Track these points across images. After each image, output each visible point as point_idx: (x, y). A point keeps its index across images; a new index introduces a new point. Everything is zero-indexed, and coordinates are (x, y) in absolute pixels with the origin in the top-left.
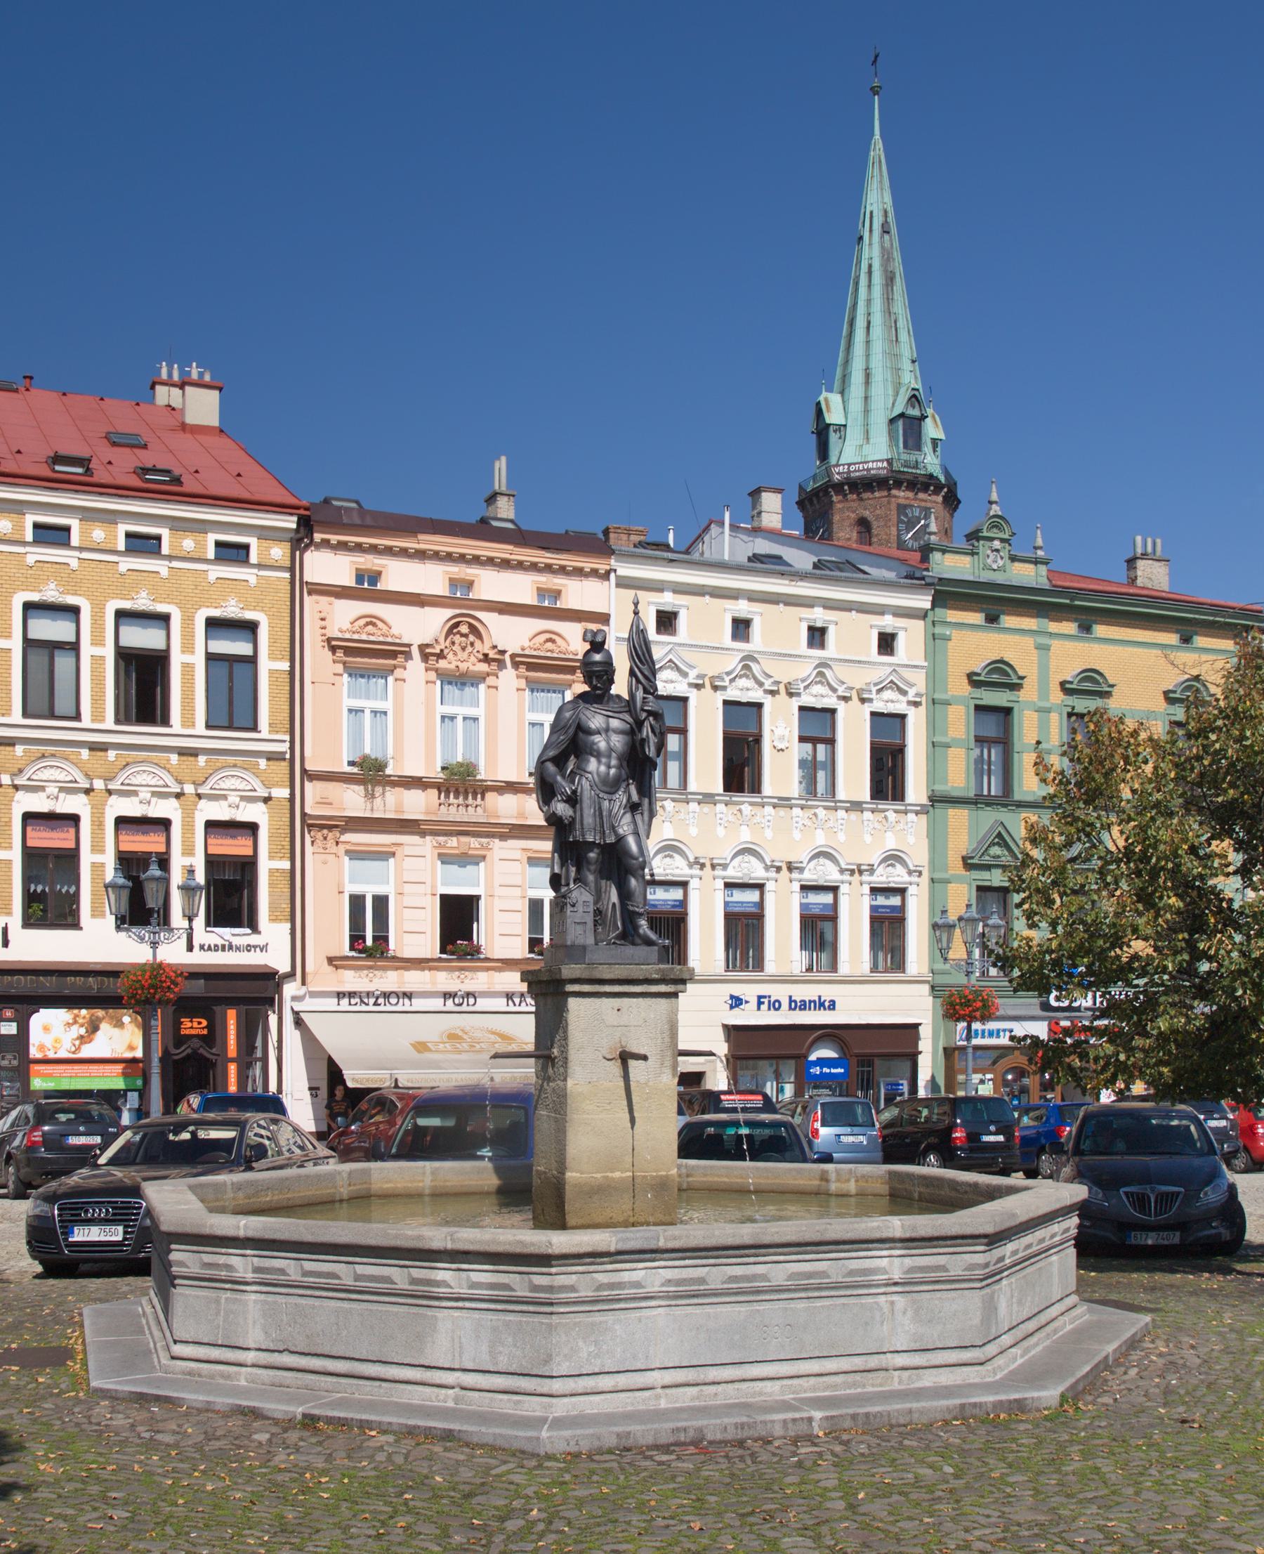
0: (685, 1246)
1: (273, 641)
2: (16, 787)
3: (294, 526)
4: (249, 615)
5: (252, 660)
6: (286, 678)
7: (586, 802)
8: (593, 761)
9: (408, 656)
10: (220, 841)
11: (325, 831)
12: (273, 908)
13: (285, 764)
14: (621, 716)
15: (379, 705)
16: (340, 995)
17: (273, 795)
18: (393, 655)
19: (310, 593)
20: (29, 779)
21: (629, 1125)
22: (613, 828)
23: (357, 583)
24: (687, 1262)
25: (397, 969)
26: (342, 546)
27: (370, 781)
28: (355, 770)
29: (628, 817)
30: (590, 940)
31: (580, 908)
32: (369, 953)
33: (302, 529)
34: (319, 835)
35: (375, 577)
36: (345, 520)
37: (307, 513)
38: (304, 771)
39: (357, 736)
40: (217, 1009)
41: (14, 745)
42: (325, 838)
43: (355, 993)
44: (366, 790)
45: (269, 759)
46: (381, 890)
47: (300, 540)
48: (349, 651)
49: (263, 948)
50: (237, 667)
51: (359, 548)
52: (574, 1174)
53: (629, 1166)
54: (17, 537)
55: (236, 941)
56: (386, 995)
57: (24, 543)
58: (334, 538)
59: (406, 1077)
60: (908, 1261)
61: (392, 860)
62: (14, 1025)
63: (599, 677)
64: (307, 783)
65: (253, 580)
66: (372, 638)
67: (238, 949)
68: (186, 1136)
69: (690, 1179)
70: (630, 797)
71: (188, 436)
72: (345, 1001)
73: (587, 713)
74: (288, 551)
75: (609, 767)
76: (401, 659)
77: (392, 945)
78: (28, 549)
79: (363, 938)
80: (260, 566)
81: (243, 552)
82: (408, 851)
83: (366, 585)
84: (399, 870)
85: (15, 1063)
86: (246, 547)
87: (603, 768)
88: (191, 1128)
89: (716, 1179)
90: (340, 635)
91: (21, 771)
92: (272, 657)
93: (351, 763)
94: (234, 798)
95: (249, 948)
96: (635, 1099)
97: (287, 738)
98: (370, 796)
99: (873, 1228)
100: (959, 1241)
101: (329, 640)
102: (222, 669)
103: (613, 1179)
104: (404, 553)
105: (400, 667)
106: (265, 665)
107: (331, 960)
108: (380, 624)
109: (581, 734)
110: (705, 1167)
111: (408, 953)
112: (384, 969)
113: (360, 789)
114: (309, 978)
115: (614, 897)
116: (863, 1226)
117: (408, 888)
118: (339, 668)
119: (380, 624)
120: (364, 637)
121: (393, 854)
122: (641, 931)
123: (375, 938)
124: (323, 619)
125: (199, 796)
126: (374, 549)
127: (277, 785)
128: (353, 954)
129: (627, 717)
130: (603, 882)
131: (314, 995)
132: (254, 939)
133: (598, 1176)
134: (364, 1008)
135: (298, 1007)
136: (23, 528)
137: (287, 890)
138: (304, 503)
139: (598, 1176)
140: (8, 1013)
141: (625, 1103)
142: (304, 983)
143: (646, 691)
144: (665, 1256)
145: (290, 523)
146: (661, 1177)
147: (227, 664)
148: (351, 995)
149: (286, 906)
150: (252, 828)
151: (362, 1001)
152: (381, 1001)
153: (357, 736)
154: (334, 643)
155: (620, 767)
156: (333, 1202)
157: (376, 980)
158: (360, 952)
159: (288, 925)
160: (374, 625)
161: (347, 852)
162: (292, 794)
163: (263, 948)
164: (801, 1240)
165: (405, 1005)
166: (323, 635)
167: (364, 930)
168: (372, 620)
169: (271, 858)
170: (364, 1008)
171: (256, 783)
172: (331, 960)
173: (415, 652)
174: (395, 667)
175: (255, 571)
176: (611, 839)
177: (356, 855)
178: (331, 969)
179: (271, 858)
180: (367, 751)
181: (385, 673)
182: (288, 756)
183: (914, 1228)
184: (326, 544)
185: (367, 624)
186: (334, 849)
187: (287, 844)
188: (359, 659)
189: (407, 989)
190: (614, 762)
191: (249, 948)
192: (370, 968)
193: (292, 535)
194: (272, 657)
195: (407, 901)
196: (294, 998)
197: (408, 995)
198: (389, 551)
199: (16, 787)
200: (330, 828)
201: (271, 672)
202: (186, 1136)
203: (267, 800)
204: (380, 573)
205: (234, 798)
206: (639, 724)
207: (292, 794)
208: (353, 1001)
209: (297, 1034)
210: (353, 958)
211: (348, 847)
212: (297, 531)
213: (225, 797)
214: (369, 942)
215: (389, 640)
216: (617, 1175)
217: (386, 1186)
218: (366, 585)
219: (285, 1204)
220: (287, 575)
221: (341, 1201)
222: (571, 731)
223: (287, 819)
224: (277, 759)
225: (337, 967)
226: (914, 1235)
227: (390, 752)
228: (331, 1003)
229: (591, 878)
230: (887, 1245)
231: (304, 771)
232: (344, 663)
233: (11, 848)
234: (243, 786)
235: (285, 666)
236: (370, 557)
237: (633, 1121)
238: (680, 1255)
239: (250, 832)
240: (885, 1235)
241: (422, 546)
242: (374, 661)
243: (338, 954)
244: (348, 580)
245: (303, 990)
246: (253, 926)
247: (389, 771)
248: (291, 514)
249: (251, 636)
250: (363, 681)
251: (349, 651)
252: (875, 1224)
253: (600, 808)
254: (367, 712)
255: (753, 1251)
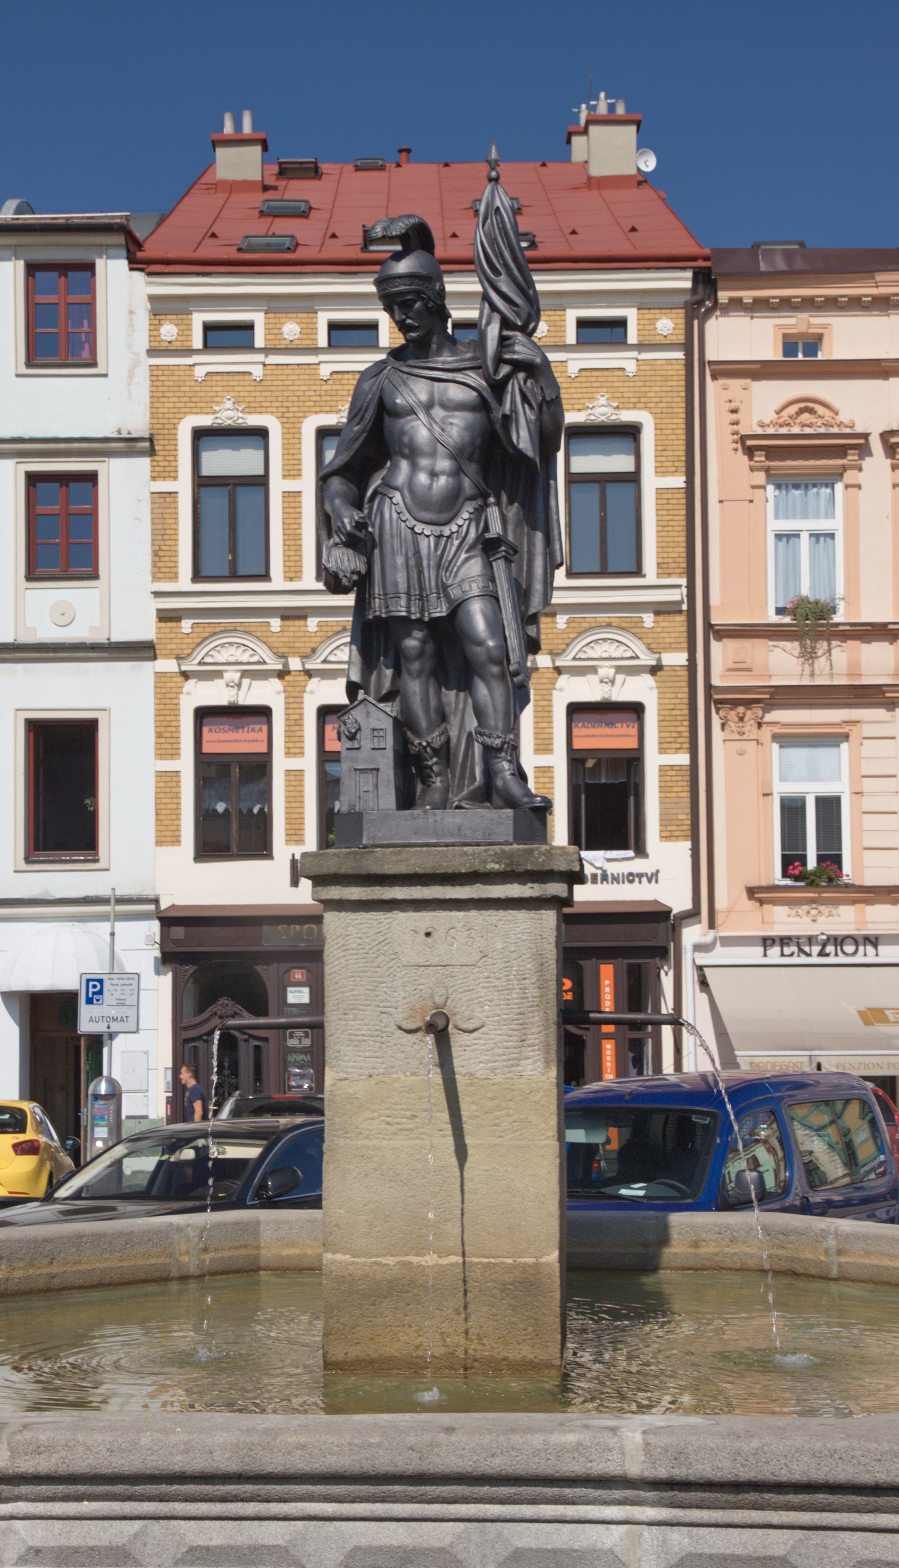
0: (63, 1469)
1: (661, 448)
2: (309, 674)
3: (688, 284)
4: (627, 416)
5: (633, 479)
6: (681, 498)
7: (391, 543)
8: (404, 465)
9: (864, 450)
10: (591, 731)
11: (741, 709)
12: (664, 821)
13: (681, 619)
14: (459, 377)
15: (822, 525)
16: (767, 942)
17: (665, 662)
18: (841, 451)
19: (714, 377)
20: (325, 661)
21: (454, 1161)
22: (443, 588)
23: (785, 354)
24: (87, 1507)
25: (854, 902)
26: (761, 306)
27: (807, 634)
28: (787, 620)
29: (475, 567)
30: (388, 799)
31: (366, 741)
32: (809, 880)
33: (701, 288)
34: (732, 715)
35: (813, 343)
36: (763, 267)
37: (707, 264)
38: (708, 626)
39: (790, 571)
40: (586, 964)
41: (305, 618)
42: (741, 719)
43: (789, 938)
44: (803, 646)
45: (657, 613)
46: (828, 789)
47: (700, 303)
48: (772, 452)
49: (653, 877)
50: (611, 488)
51: (786, 305)
52: (339, 1257)
53: (455, 1243)
54: (307, 343)
55: (613, 869)
56: (839, 941)
57: (315, 350)
58: (748, 295)
59: (834, 1060)
60: (679, 1538)
61: (844, 746)
62: (306, 990)
63: (406, 306)
64: (715, 645)
65: (631, 367)
66: (808, 430)
67: (616, 879)
68: (188, 1154)
69: (843, 1259)
70: (486, 529)
71: (595, 193)
72: (775, 951)
73: (396, 378)
74: (681, 321)
75: (433, 475)
76: (852, 456)
77: (847, 867)
78: (322, 357)
79: (803, 859)
80: (641, 347)
81: (618, 331)
82: (867, 730)
83: (800, 357)
84: (855, 760)
85: (307, 1042)
86: (621, 323)
87: (423, 478)
88: (200, 1142)
89: (886, 1262)
90: (759, 431)
91: (314, 650)
92: (660, 471)
93: (780, 611)
94: (607, 671)
95: (631, 878)
96: (466, 1110)
97: (683, 581)
98: (809, 655)
99: (562, 1451)
100: (822, 1498)
101: (743, 439)
102: (591, 494)
103: (420, 1266)
104: (855, 304)
105: (852, 467)
106: (650, 483)
107: (752, 892)
108: (820, 410)
109: (387, 419)
110: (866, 1237)
111: (871, 879)
112: (836, 902)
113: (793, 646)
114: (719, 919)
115: (472, 723)
116: (537, 1440)
117: (868, 785)
118: (760, 478)
119: (820, 410)
120: (796, 430)
121: (846, 737)
122: (499, 783)
123: (820, 859)
124: (734, 411)
125: (559, 670)
126: (809, 304)
127: (670, 648)
128: (788, 882)
129: (474, 379)
130: (450, 696)
131: (728, 942)
132: (638, 865)
133: (390, 1261)
134: (804, 960)
135: (702, 959)
136: (314, 331)
137: (686, 795)
138: (707, 251)
139: (390, 1261)
140: (298, 975)
141: (446, 1116)
142: (712, 925)
143: (506, 323)
144: (24, 1489)
145: (683, 281)
146: (524, 1267)
147: (596, 487)
148: (784, 941)
149: (685, 817)
150: (636, 710)
151: (801, 950)
152: (830, 949)
153: (790, 571)
154: (750, 443)
155: (457, 472)
156: (164, 1279)
157: (821, 919)
158: (797, 878)
159: (688, 844)
160: (811, 411)
161: (776, 737)
162: (692, 659)
163: (653, 877)
164: (367, 1467)
165: (869, 954)
166: (735, 433)
167: (804, 848)
168: (807, 405)
169: (662, 750)
170: (804, 960)
171: (639, 648)
172: (752, 892)
173: (876, 444)
174: (845, 468)
175: (634, 354)
176: (440, 610)
177: (785, 740)
178: (755, 904)
179: (662, 750)
180: (805, 590)
181: (830, 479)
182: (685, 607)
183: (679, 1455)
184: (736, 305)
185: (801, 411)
186: (754, 733)
187: (685, 729)
188: (789, 463)
189: (871, 930)
190: (444, 464)
191: (631, 878)
192: (812, 901)
193: (687, 297)
194: (660, 471)
195: (868, 803)
196: (698, 948)
197: (873, 941)
198: (832, 304)
199: (309, 674)
200: (748, 703)
201: (660, 491)
202: (188, 1154)
203: (655, 670)
204: (820, 337)
205: (607, 671)
206: (498, 388)
207: (692, 659)
208: (787, 950)
209: (704, 997)
210: (786, 888)
211: (776, 730)
212: (694, 290)
213: (594, 670)
214: (812, 863)
215: (835, 430)
216: (430, 1260)
217: (286, 1252)
218: (800, 357)
219: (41, 1284)
220: (680, 355)
221: (184, 1278)
222: (369, 415)
223: (684, 695)
224: (669, 613)
225: (761, 902)
226: (680, 1472)
227: (840, 591)
228: (754, 954)
229: (414, 687)
230: (618, 1494)
231: (708, 626)
232: (767, 470)
233: (302, 754)
234: (619, 652)
235: (679, 481)
236: (803, 316)
237: (461, 1153)
238: (61, 1489)
239: (634, 716)
240: (598, 1467)
241: (883, 291)
242: (812, 462)
243: (763, 883)
244: (771, 351)
245: (710, 936)
246: (641, 851)
247: (837, 618)
248: (683, 269)
249: (632, 446)
250: (797, 493)
251: (772, 452)
252: (571, 1438)
253: (417, 553)
254: (805, 536)
255: (248, 1488)
